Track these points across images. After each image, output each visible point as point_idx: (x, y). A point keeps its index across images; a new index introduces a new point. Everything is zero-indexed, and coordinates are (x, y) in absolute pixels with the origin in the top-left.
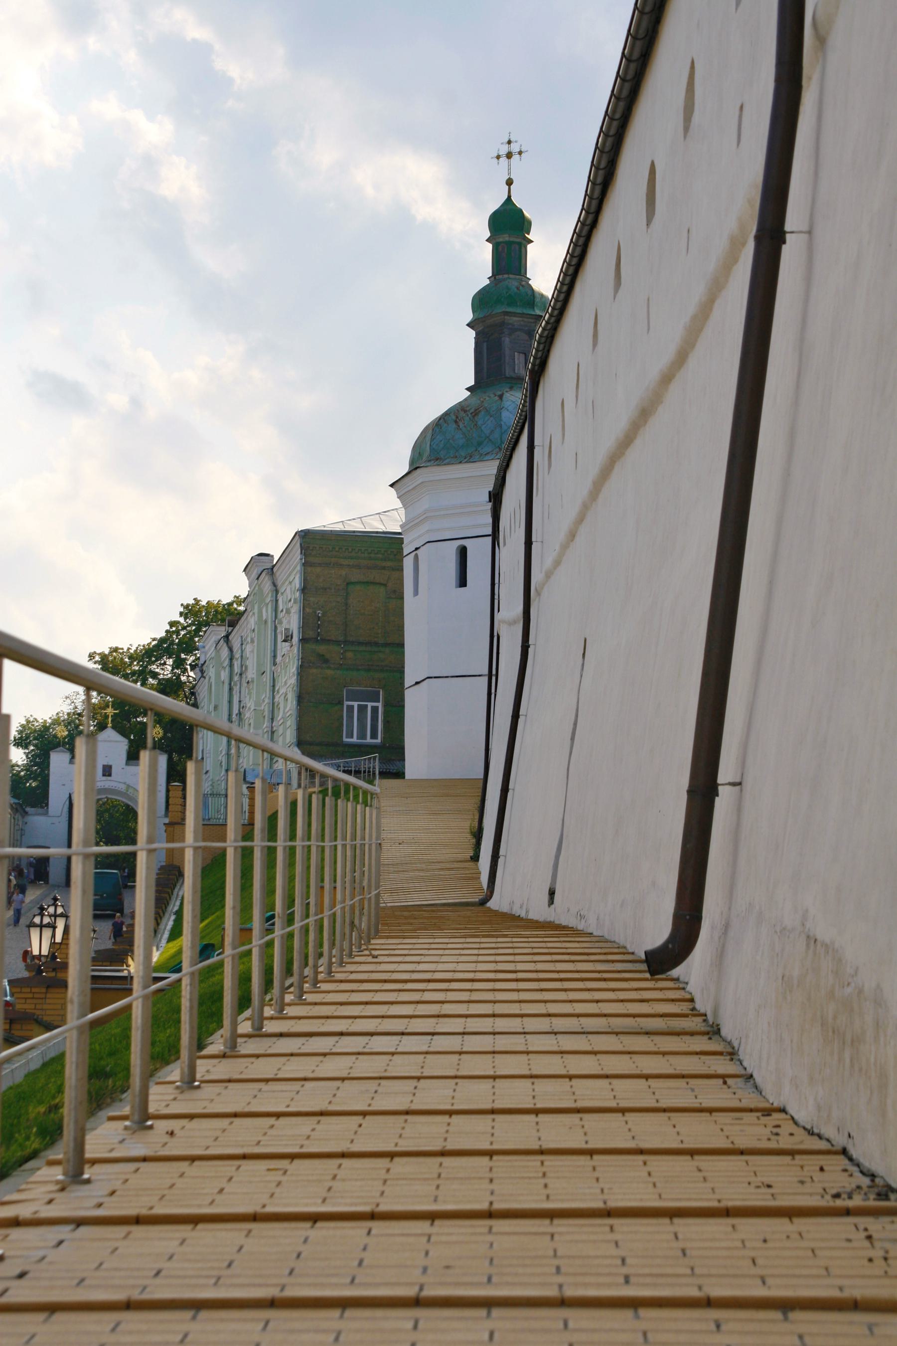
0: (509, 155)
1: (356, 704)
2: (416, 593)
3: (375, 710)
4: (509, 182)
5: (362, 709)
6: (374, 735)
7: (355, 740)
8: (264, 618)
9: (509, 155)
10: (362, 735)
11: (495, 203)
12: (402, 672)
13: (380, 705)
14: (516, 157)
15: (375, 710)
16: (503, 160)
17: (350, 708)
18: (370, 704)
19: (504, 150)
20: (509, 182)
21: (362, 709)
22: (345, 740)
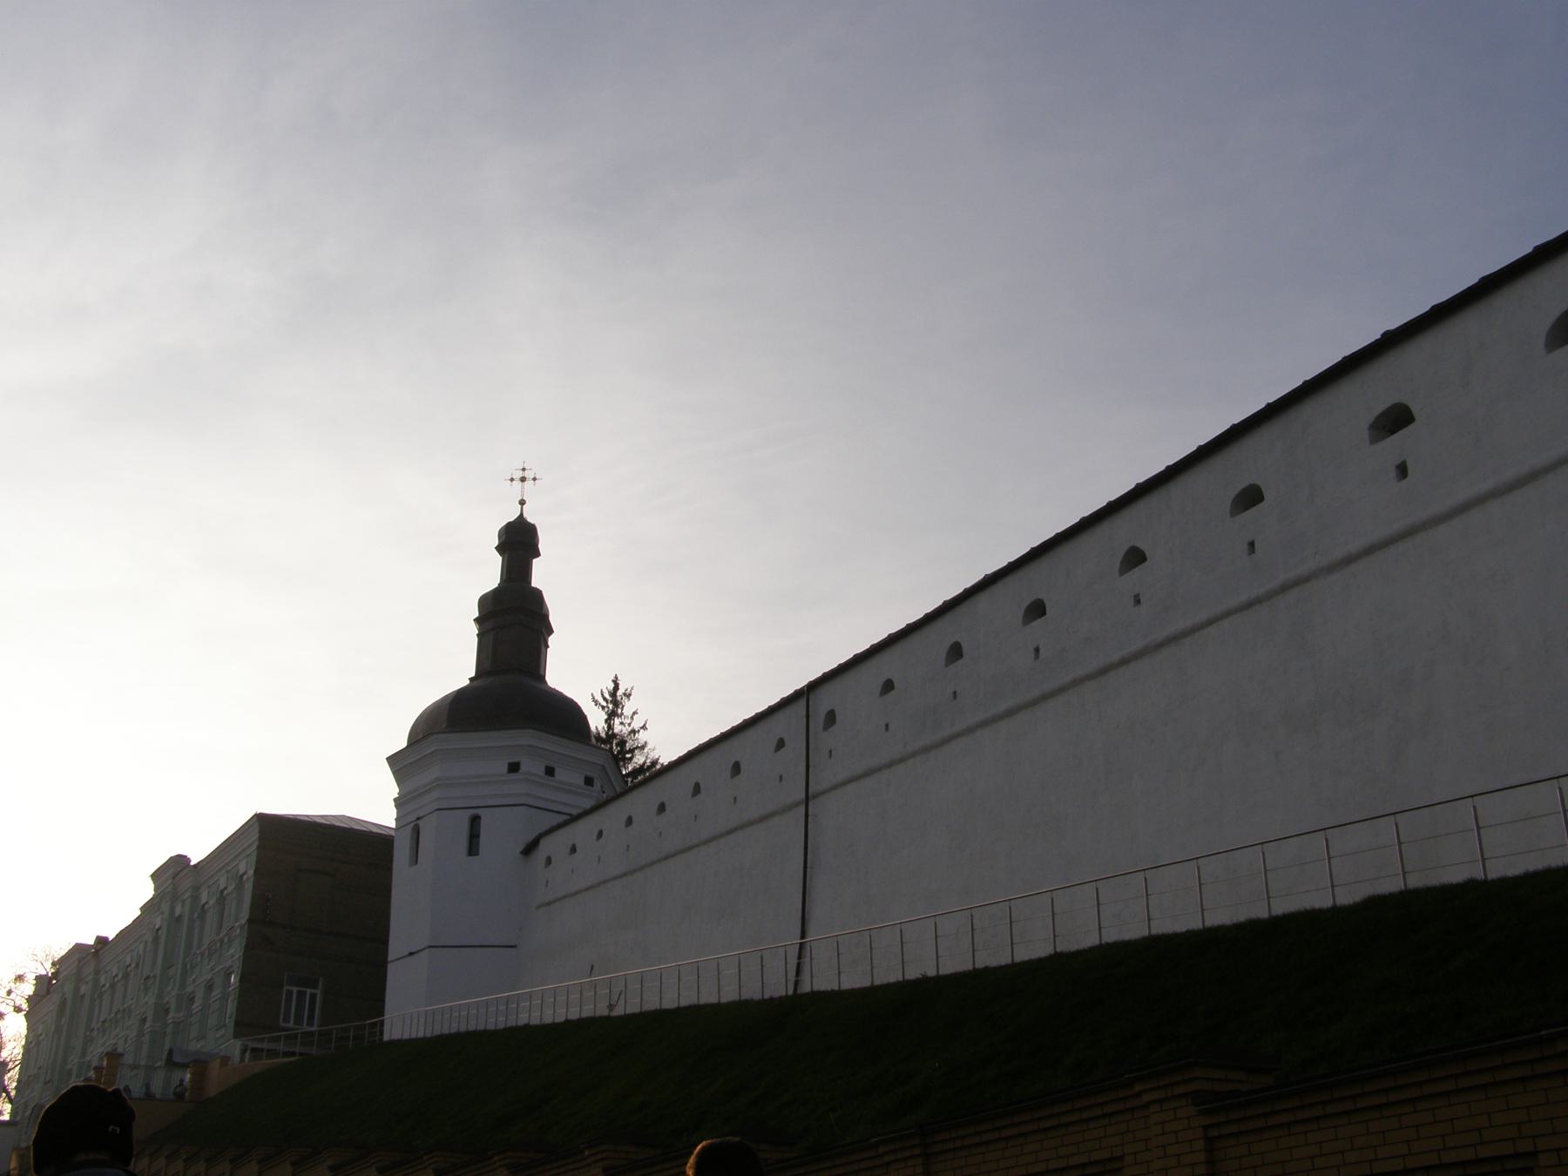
0: (523, 479)
1: (295, 989)
2: (415, 859)
3: (313, 997)
4: (522, 503)
5: (301, 995)
6: (310, 1023)
7: (291, 1024)
8: (177, 913)
9: (523, 479)
10: (298, 1021)
11: (512, 516)
12: (385, 942)
13: (318, 992)
14: (529, 483)
15: (313, 997)
16: (517, 483)
17: (290, 993)
18: (309, 991)
19: (520, 474)
20: (522, 503)
21: (301, 995)
22: (282, 1024)
